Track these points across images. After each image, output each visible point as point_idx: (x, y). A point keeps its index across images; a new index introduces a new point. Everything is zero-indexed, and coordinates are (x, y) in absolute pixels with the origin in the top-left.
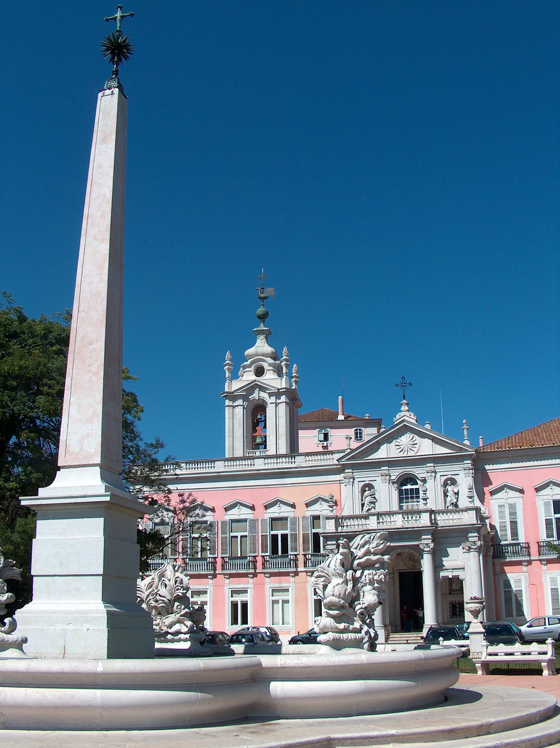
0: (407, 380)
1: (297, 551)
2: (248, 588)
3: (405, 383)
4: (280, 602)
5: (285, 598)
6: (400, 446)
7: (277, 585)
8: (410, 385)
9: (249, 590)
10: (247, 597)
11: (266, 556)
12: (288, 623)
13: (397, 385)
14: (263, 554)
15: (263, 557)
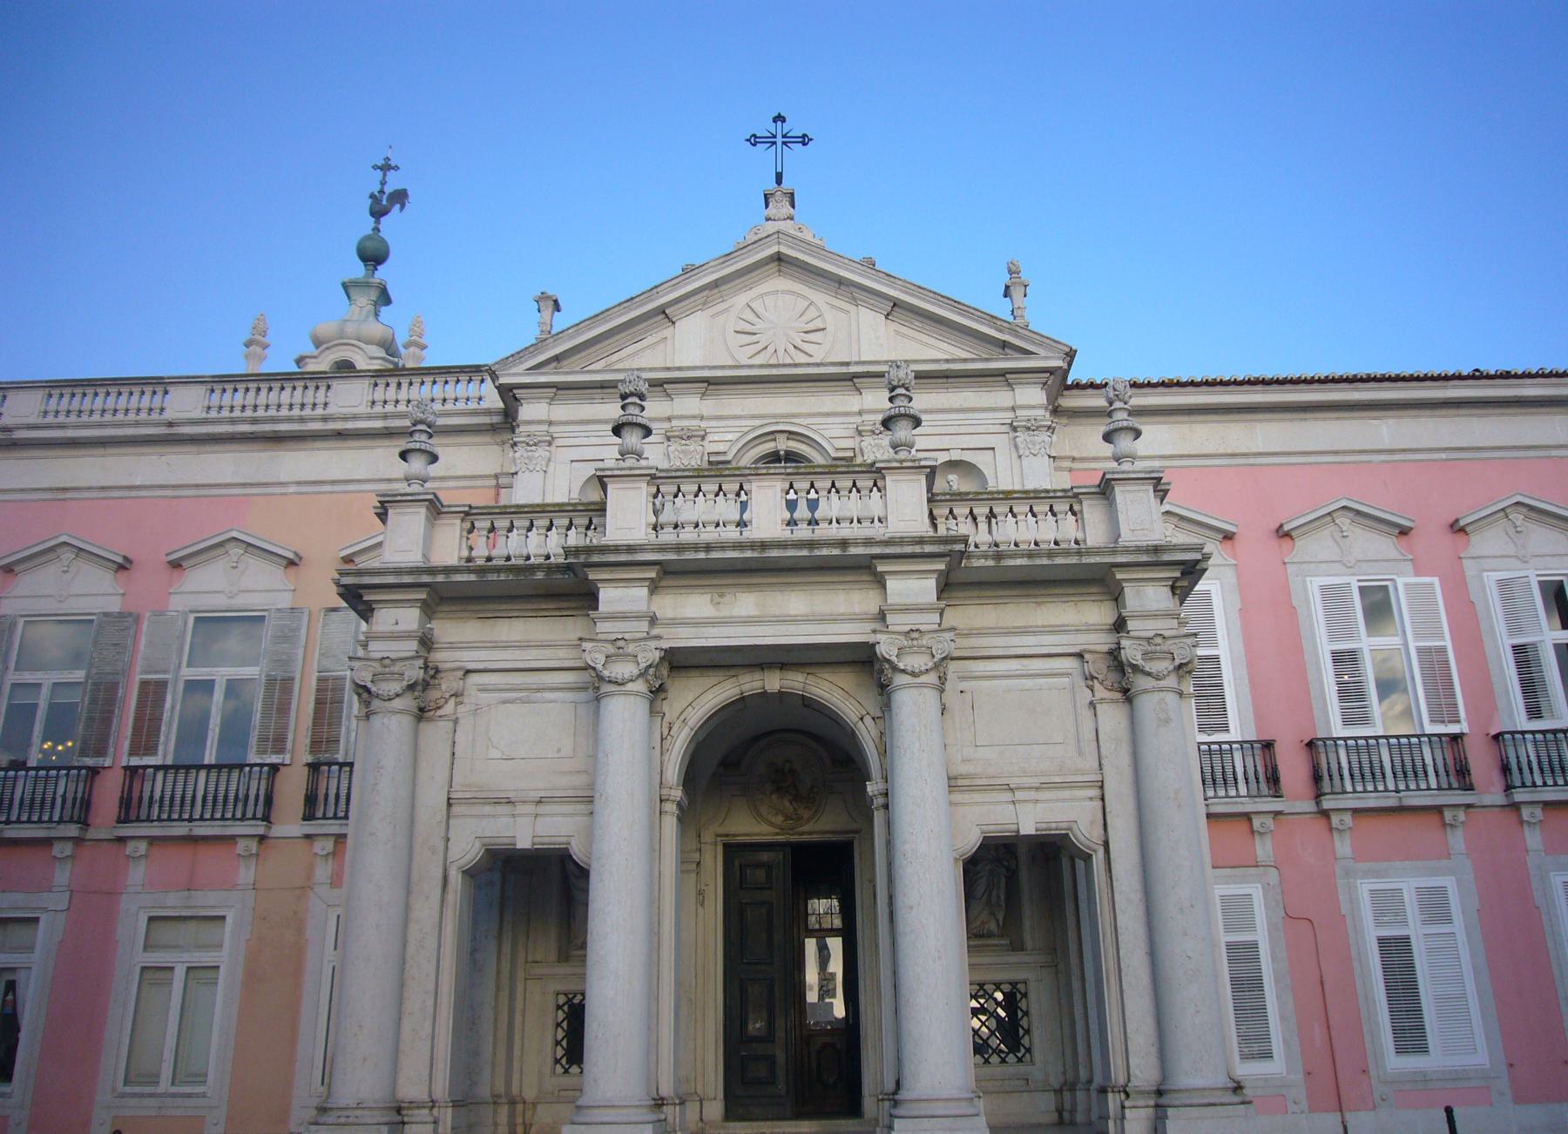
0: (795, 127)
1: (281, 751)
2: (45, 910)
3: (784, 136)
4: (180, 973)
5: (206, 958)
6: (754, 338)
7: (173, 903)
8: (804, 144)
9: (43, 917)
10: (30, 948)
11: (145, 767)
12: (201, 1078)
13: (754, 140)
14: (135, 761)
15: (132, 771)
